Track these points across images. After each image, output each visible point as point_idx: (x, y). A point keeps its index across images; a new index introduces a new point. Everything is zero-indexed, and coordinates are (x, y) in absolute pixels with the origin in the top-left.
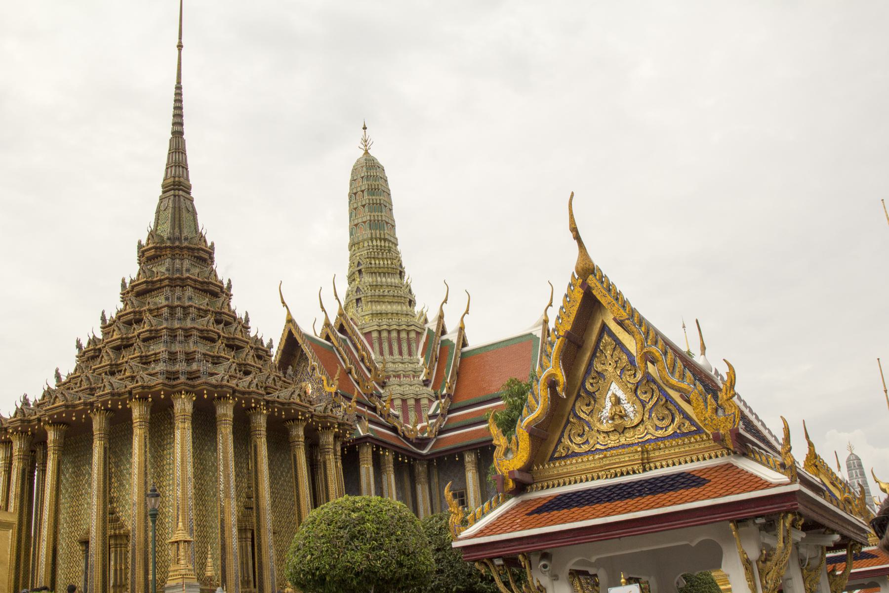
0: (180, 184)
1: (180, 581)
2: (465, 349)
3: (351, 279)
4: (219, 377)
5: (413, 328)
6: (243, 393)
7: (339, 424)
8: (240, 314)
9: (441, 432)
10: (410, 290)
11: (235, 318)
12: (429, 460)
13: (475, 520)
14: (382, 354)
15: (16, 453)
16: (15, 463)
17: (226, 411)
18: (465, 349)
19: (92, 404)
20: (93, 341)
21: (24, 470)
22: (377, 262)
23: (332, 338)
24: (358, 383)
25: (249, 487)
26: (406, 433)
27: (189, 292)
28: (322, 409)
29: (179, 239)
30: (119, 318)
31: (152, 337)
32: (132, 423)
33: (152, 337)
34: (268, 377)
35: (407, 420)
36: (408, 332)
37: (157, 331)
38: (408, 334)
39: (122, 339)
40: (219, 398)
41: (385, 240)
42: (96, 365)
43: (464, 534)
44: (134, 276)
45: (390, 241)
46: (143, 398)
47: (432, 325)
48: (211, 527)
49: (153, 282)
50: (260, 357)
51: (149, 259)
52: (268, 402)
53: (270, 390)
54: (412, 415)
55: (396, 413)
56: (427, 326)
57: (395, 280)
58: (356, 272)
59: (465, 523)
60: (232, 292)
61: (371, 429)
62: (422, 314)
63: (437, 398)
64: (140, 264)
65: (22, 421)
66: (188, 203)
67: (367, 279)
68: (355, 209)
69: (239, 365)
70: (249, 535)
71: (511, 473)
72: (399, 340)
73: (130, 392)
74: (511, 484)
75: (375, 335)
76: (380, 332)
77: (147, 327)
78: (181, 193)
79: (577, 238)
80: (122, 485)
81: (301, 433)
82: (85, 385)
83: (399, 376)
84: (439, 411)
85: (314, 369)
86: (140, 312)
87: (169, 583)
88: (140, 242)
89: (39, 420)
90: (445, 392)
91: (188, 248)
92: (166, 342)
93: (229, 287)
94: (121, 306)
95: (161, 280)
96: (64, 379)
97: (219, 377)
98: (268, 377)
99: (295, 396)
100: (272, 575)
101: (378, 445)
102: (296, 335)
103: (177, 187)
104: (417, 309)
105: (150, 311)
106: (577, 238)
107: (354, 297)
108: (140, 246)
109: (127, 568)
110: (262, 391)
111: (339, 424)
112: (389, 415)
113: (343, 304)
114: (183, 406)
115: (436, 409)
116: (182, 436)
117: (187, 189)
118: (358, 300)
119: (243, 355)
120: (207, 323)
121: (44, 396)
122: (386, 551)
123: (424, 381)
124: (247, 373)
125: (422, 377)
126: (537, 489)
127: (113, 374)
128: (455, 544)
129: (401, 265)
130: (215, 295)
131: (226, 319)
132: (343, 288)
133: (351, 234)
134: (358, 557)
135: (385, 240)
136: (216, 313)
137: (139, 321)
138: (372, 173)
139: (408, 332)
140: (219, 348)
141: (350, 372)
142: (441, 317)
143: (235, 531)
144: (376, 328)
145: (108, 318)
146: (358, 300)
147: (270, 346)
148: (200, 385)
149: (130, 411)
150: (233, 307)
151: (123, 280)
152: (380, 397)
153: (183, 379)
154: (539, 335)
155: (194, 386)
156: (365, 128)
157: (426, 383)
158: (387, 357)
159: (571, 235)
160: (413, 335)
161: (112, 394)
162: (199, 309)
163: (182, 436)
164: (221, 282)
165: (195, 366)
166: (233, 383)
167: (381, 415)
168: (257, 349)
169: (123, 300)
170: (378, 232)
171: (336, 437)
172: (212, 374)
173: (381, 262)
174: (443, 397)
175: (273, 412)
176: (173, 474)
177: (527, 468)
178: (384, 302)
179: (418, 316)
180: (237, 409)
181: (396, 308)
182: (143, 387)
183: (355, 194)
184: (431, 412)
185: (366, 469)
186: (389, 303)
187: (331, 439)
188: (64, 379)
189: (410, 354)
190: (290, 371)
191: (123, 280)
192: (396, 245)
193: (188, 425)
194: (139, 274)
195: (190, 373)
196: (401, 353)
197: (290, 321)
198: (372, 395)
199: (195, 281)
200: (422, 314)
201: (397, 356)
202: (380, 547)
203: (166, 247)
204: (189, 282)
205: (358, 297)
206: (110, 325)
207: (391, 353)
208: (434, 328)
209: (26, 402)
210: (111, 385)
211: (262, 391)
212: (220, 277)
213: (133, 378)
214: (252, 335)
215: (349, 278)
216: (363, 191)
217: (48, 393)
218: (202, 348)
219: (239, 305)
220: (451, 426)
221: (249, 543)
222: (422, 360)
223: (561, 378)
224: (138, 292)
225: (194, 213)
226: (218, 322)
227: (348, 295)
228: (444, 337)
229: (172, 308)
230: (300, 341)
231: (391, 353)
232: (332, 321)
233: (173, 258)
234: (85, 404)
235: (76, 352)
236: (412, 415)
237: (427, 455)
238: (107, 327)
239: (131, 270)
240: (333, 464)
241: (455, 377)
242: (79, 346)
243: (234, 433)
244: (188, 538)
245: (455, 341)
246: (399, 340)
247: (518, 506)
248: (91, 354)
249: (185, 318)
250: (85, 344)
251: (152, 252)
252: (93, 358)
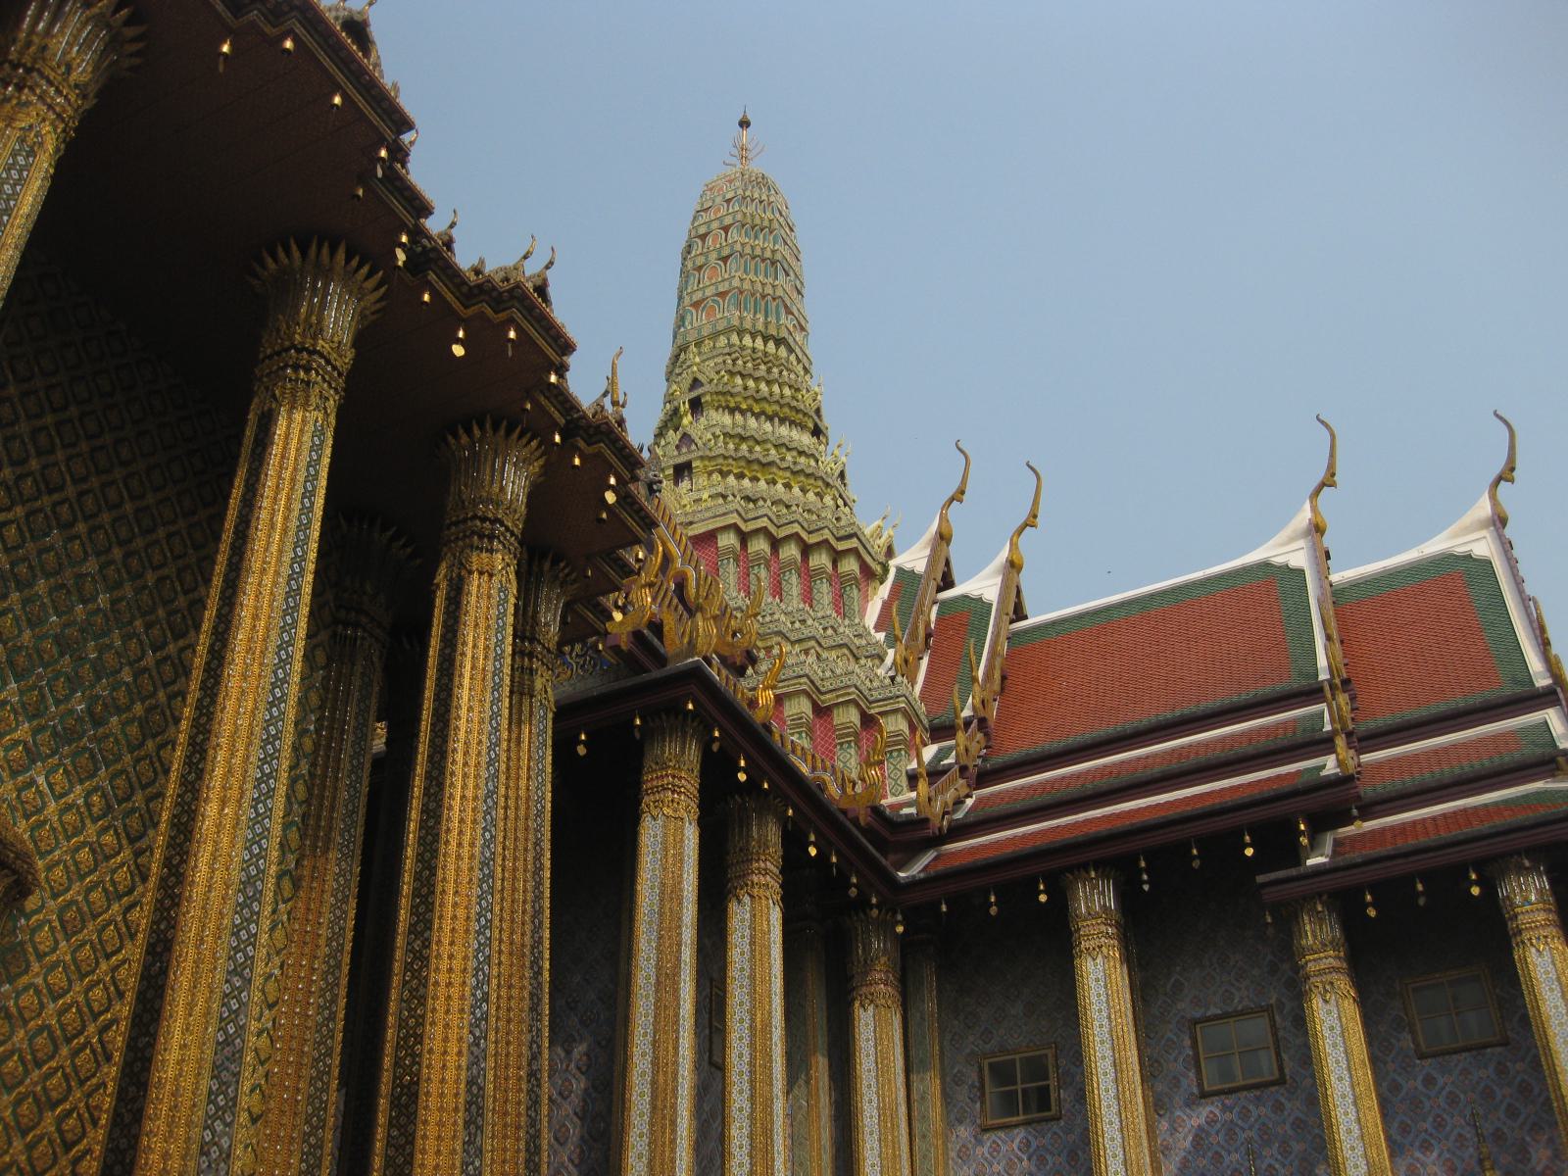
5: (853, 543)
10: (842, 475)
12: (916, 903)
22: (751, 383)
26: (834, 790)
36: (837, 556)
38: (835, 563)
41: (779, 342)
45: (791, 350)
63: (941, 731)
68: (700, 268)
75: (728, 540)
84: (951, 760)
90: (967, 713)
129: (818, 411)
139: (837, 556)
144: (733, 519)
156: (744, 124)
160: (850, 565)
170: (761, 317)
173: (763, 386)
183: (703, 237)
205: (681, 460)
216: (726, 229)
237: (914, 884)
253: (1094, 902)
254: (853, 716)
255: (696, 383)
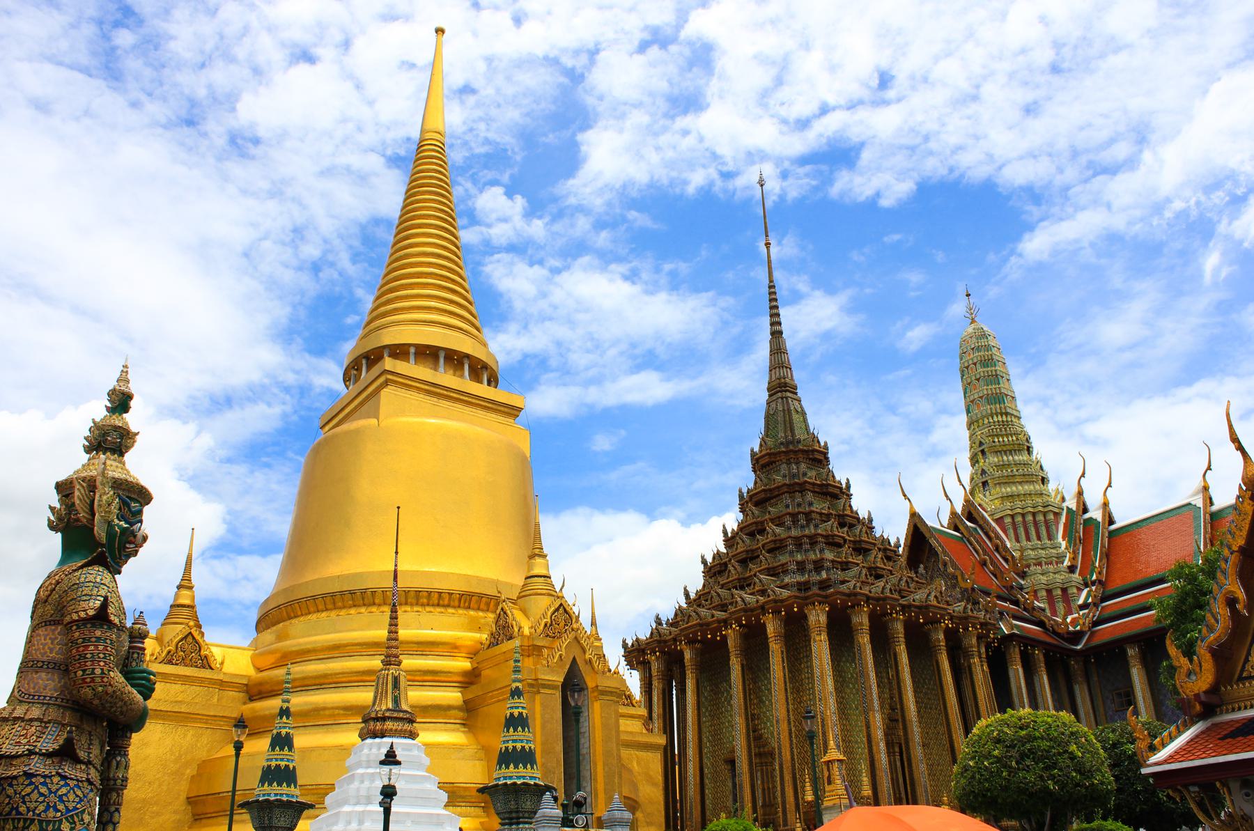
0: (786, 385)
1: (837, 801)
2: (1113, 527)
3: (974, 461)
4: (851, 585)
6: (878, 599)
7: (981, 624)
8: (863, 514)
9: (1096, 624)
11: (858, 519)
13: (1164, 745)
14: (1018, 540)
15: (654, 673)
16: (655, 683)
17: (861, 619)
18: (1113, 527)
19: (726, 623)
20: (718, 555)
21: (664, 690)
23: (961, 527)
24: (995, 576)
25: (891, 698)
27: (809, 496)
28: (961, 608)
29: (792, 442)
30: (742, 528)
31: (777, 547)
32: (767, 638)
33: (777, 547)
34: (900, 580)
35: (1054, 613)
36: (1045, 514)
37: (781, 540)
39: (747, 551)
40: (853, 607)
41: (1007, 414)
42: (722, 580)
43: (1153, 759)
44: (751, 486)
46: (776, 612)
47: (1071, 503)
48: (857, 742)
49: (770, 490)
50: (889, 558)
51: (763, 466)
52: (903, 607)
53: (904, 593)
54: (1060, 607)
55: (1042, 605)
56: (1064, 505)
57: (1023, 457)
58: (979, 452)
59: (1153, 749)
60: (852, 491)
61: (1018, 627)
62: (1058, 492)
63: (1086, 585)
64: (755, 471)
65: (659, 642)
66: (796, 403)
67: (993, 459)
69: (869, 569)
70: (897, 749)
71: (1197, 696)
72: (1036, 523)
73: (762, 607)
74: (1198, 707)
76: (1013, 517)
77: (771, 538)
78: (789, 394)
79: (1240, 448)
80: (761, 701)
81: (941, 636)
82: (716, 601)
83: (1040, 564)
85: (945, 564)
86: (762, 523)
87: (826, 804)
88: (752, 450)
89: (675, 640)
90: (1094, 577)
91: (802, 451)
92: (791, 553)
93: (848, 486)
94: (741, 516)
95: (778, 487)
96: (693, 596)
97: (851, 585)
98: (900, 580)
99: (932, 597)
100: (926, 791)
101: (1025, 642)
102: (923, 529)
103: (781, 388)
104: (1051, 487)
105: (772, 520)
106: (1240, 448)
107: (979, 480)
108: (753, 454)
109: (774, 787)
110: (896, 596)
111: (981, 624)
112: (1034, 608)
113: (968, 488)
114: (818, 617)
115: (1087, 598)
116: (821, 647)
117: (793, 389)
118: (985, 484)
119: (871, 558)
120: (830, 527)
121: (676, 615)
122: (1060, 770)
123: (1069, 567)
124: (878, 577)
125: (1067, 563)
126: (1227, 712)
127: (742, 588)
128: (1144, 771)
130: (835, 497)
131: (849, 520)
132: (966, 472)
133: (968, 412)
134: (1031, 777)
135: (1007, 414)
136: (839, 516)
137: (762, 531)
138: (983, 342)
139: (1045, 514)
140: (846, 553)
141: (984, 564)
142: (1080, 493)
143: (882, 745)
145: (729, 531)
146: (985, 484)
147: (898, 545)
148: (832, 594)
149: (764, 625)
150: (855, 508)
151: (740, 491)
152: (1021, 588)
153: (815, 590)
154: (1200, 503)
155: (826, 597)
156: (968, 295)
157: (1072, 569)
158: (1024, 543)
159: (1232, 446)
160: (1051, 516)
161: (745, 610)
162: (821, 514)
163: (821, 647)
164: (840, 482)
165: (824, 575)
166: (865, 590)
167: (1025, 609)
168: (885, 550)
169: (742, 510)
171: (979, 638)
172: (843, 582)
174: (1093, 583)
175: (910, 616)
176: (813, 688)
177: (1214, 690)
178: (1014, 483)
179: (1053, 494)
180: (873, 617)
181: (1028, 488)
182: (775, 601)
184: (1081, 602)
185: (1017, 672)
186: (1020, 483)
187: (974, 641)
188: (693, 596)
189: (1050, 537)
190: (921, 569)
191: (740, 491)
192: (1019, 418)
193: (824, 636)
194: (756, 483)
195: (821, 582)
196: (1039, 538)
197: (914, 516)
198: (1012, 587)
199: (814, 484)
200: (1058, 492)
201: (1035, 542)
202: (1054, 765)
203: (780, 453)
204: (808, 486)
206: (733, 537)
207: (1028, 539)
208: (1074, 506)
209: (658, 621)
210: (743, 600)
211: (896, 596)
212: (838, 478)
213: (763, 592)
214: (878, 535)
215: (971, 459)
217: (679, 612)
218: (829, 555)
219: (861, 503)
220: (1106, 614)
221: (898, 758)
222: (1064, 544)
223: (1241, 594)
224: (752, 502)
225: (804, 414)
226: (842, 525)
227: (972, 479)
228: (1087, 516)
229: (794, 516)
230: (927, 535)
231: (1028, 539)
232: (959, 510)
233: (789, 463)
234: (719, 621)
235: (702, 567)
236: (1060, 607)
238: (729, 541)
239: (746, 479)
240: (979, 668)
241: (1105, 561)
242: (704, 562)
243: (872, 641)
244: (841, 757)
245: (1100, 519)
246: (1036, 523)
247: (1208, 729)
248: (718, 569)
249: (808, 525)
250: (709, 560)
251: (766, 459)
252: (720, 572)
253: (1131, 652)
254: (1059, 592)
255: (981, 444)
